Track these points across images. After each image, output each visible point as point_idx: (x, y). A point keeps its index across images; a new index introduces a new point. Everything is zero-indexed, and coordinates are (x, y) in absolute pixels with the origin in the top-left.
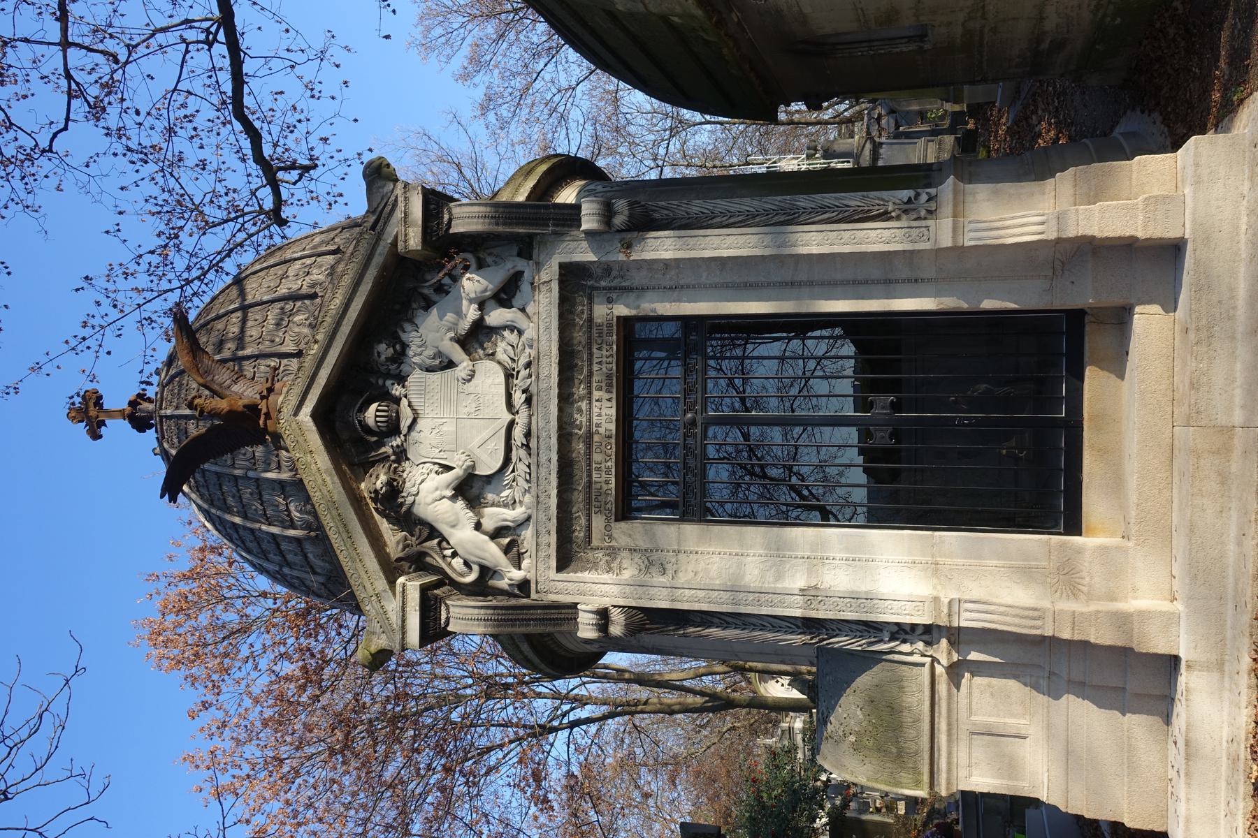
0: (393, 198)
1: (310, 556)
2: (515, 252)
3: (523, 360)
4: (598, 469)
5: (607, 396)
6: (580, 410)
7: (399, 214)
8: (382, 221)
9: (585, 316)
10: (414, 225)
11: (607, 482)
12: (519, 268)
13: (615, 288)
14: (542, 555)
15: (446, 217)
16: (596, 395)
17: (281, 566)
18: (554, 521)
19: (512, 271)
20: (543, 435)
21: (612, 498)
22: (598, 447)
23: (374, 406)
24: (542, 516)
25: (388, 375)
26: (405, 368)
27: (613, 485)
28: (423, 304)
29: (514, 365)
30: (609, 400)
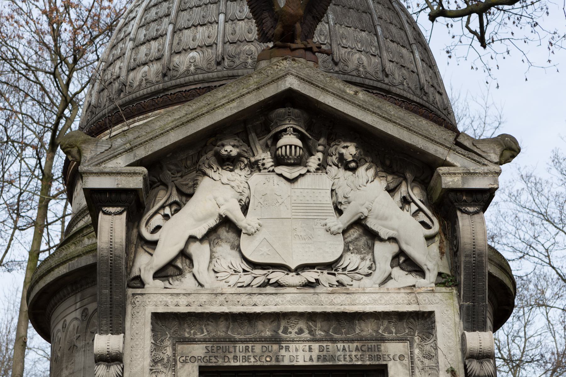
0: (486, 162)
1: (146, 68)
2: (442, 270)
4: (247, 349)
5: (315, 357)
6: (301, 331)
7: (473, 167)
8: (466, 153)
9: (386, 335)
10: (464, 181)
11: (235, 358)
12: (427, 274)
13: (412, 363)
14: (169, 299)
15: (471, 209)
16: (316, 346)
17: (133, 40)
18: (200, 310)
19: (425, 268)
20: (278, 299)
21: (220, 363)
22: (267, 348)
24: (204, 298)
26: (333, 170)
27: (233, 363)
28: (392, 186)
29: (340, 271)
30: (311, 359)
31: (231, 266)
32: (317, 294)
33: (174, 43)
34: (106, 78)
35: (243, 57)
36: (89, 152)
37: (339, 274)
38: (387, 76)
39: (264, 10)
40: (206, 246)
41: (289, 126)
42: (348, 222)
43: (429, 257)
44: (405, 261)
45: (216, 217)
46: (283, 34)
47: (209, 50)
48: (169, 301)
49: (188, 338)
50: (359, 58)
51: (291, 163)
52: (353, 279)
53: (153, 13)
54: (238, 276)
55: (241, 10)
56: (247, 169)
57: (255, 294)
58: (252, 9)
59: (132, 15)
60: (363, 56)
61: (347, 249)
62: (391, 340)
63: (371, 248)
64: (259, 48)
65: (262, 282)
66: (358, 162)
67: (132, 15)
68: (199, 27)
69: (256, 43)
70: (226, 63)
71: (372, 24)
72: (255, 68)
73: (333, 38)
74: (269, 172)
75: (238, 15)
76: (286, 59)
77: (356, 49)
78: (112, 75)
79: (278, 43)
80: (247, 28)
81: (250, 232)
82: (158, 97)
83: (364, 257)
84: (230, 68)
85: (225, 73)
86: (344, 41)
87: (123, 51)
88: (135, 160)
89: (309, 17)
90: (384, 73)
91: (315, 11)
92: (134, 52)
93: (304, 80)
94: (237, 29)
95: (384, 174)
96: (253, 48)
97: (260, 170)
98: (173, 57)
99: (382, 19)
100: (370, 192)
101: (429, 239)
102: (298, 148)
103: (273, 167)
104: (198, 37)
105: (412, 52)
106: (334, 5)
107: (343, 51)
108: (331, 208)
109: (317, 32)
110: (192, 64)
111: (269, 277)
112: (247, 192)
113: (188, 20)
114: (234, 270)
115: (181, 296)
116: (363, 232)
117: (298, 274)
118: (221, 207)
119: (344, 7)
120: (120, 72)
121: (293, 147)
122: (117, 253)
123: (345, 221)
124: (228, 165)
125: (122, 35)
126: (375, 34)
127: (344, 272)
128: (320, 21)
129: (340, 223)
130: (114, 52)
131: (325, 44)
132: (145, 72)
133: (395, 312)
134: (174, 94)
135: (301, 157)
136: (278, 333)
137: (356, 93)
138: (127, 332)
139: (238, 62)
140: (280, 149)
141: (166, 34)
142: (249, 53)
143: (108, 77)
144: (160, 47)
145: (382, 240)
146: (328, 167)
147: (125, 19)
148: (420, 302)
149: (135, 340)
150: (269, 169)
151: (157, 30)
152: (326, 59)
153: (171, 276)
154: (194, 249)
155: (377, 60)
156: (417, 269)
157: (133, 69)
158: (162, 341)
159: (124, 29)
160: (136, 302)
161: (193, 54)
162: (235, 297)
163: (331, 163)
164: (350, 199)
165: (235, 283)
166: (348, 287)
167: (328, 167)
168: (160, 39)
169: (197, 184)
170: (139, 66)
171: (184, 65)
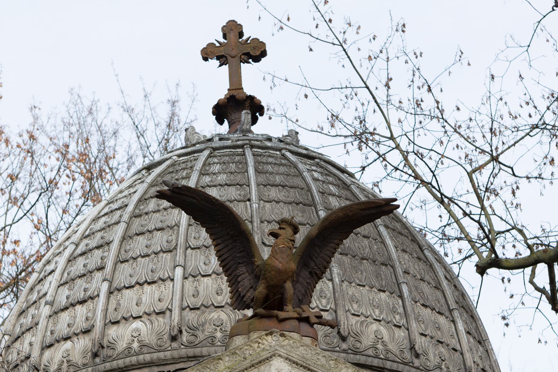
1: (68, 344)
17: (51, 304)
33: (110, 308)
34: (10, 358)
35: (209, 329)
38: (417, 356)
39: (239, 263)
46: (266, 298)
47: (161, 319)
50: (376, 331)
53: (79, 266)
55: (207, 262)
58: (222, 262)
59: (49, 268)
60: (382, 328)
64: (232, 316)
67: (49, 268)
68: (146, 286)
69: (228, 309)
70: (185, 337)
71: (394, 281)
72: (226, 346)
73: (340, 302)
75: (203, 269)
76: (271, 334)
77: (372, 317)
78: (18, 354)
79: (260, 311)
80: (215, 287)
84: (191, 345)
85: (184, 352)
86: (355, 306)
87: (35, 320)
89: (305, 273)
90: (413, 352)
91: (312, 264)
92: (51, 320)
93: (297, 364)
94: (201, 289)
96: (223, 316)
98: (108, 329)
99: (409, 274)
104: (144, 300)
105: (453, 321)
106: (341, 254)
107: (353, 320)
109: (315, 295)
110: (136, 339)
113: (131, 276)
119: (354, 257)
120: (31, 350)
125: (34, 296)
126: (399, 296)
128: (320, 278)
130: (22, 320)
131: (327, 311)
132: (67, 350)
139: (201, 336)
141: (98, 295)
142: (217, 324)
143: (13, 357)
144: (90, 315)
147: (40, 273)
151: (85, 290)
152: (329, 331)
155: (401, 334)
157: (51, 346)
159: (38, 288)
161: (137, 324)
168: (89, 302)
170: (58, 341)
171: (123, 341)
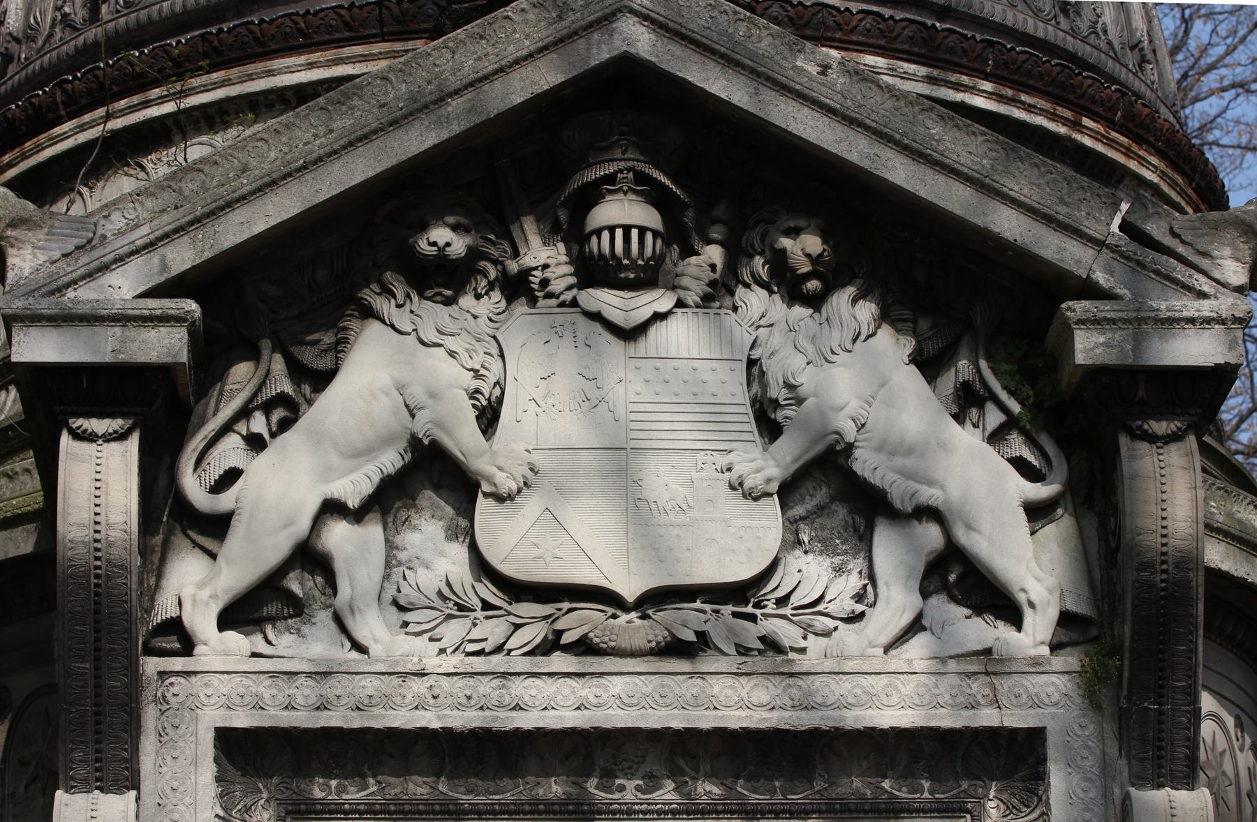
0: (1205, 285)
2: (1071, 606)
3: (787, 633)
12: (1029, 617)
14: (264, 688)
15: (1161, 427)
18: (357, 722)
19: (1022, 598)
23: (649, 217)
24: (370, 686)
25: (736, 254)
26: (755, 301)
28: (931, 348)
29: (771, 608)
31: (446, 591)
32: (702, 675)
36: (27, 252)
37: (766, 616)
40: (373, 531)
41: (622, 165)
42: (795, 460)
43: (1037, 567)
44: (962, 579)
45: (404, 444)
48: (266, 696)
49: (321, 802)
51: (627, 279)
52: (807, 630)
54: (468, 622)
56: (496, 295)
57: (519, 674)
61: (793, 542)
62: (918, 811)
63: (863, 541)
65: (538, 640)
66: (832, 275)
74: (562, 305)
81: (504, 491)
82: (221, 30)
83: (844, 563)
88: (163, 279)
95: (906, 313)
97: (533, 301)
100: (863, 375)
101: (1037, 512)
102: (649, 237)
103: (575, 291)
108: (745, 418)
111: (559, 625)
112: (496, 365)
114: (456, 604)
115: (302, 679)
116: (836, 492)
117: (644, 617)
118: (419, 415)
121: (635, 232)
122: (117, 553)
123: (788, 459)
124: (439, 286)
127: (781, 611)
129: (772, 463)
133: (931, 728)
134: (271, 22)
135: (659, 259)
136: (585, 789)
137: (825, 68)
138: (146, 785)
140: (594, 239)
145: (896, 516)
146: (740, 291)
148: (1003, 701)
149: (169, 807)
150: (562, 298)
153: (272, 620)
154: (339, 537)
156: (999, 603)
158: (247, 809)
160: (169, 695)
162: (459, 682)
163: (747, 278)
164: (802, 391)
165: (457, 641)
166: (792, 655)
167: (740, 291)
169: (345, 341)
